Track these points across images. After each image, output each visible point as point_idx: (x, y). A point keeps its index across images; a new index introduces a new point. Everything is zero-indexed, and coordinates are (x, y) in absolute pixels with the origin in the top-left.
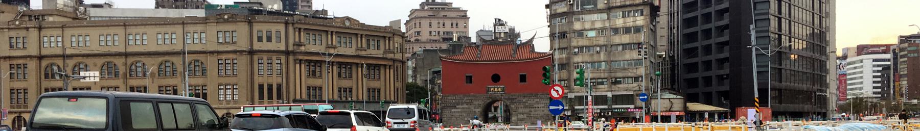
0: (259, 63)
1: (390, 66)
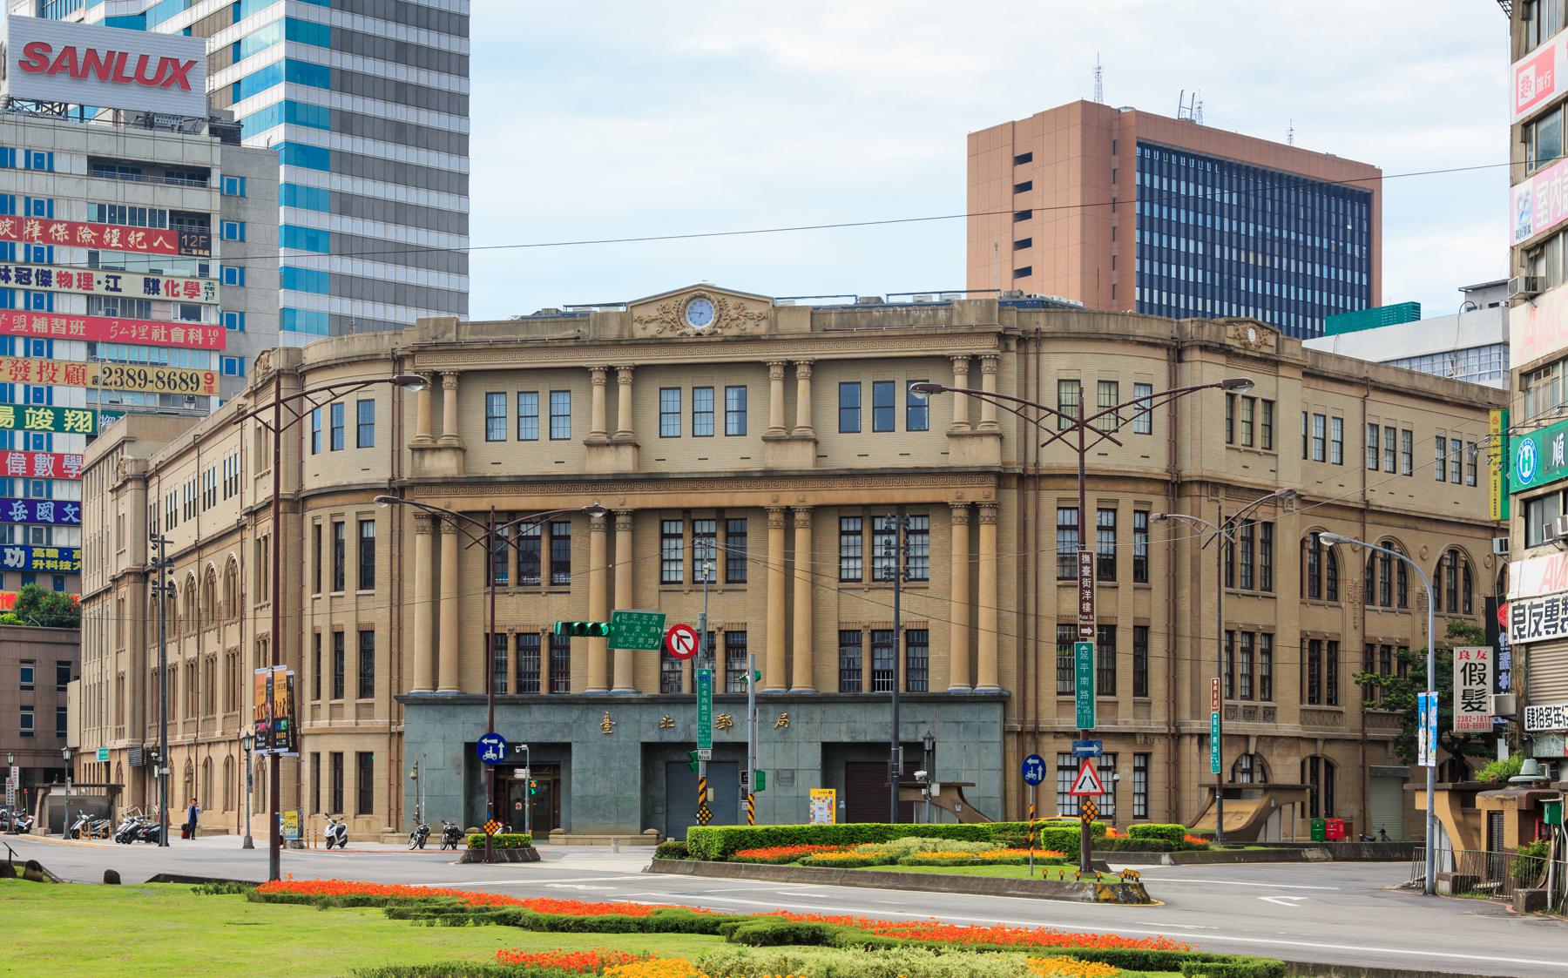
0: (842, 533)
1: (973, 509)
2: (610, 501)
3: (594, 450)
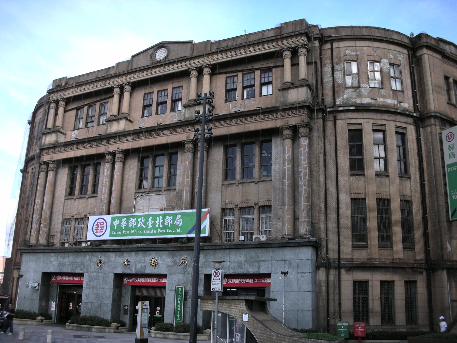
1: (295, 129)
2: (113, 148)
3: (109, 123)
